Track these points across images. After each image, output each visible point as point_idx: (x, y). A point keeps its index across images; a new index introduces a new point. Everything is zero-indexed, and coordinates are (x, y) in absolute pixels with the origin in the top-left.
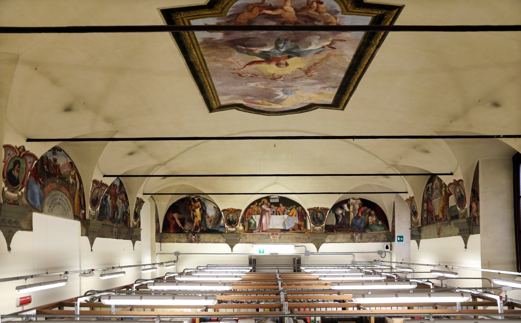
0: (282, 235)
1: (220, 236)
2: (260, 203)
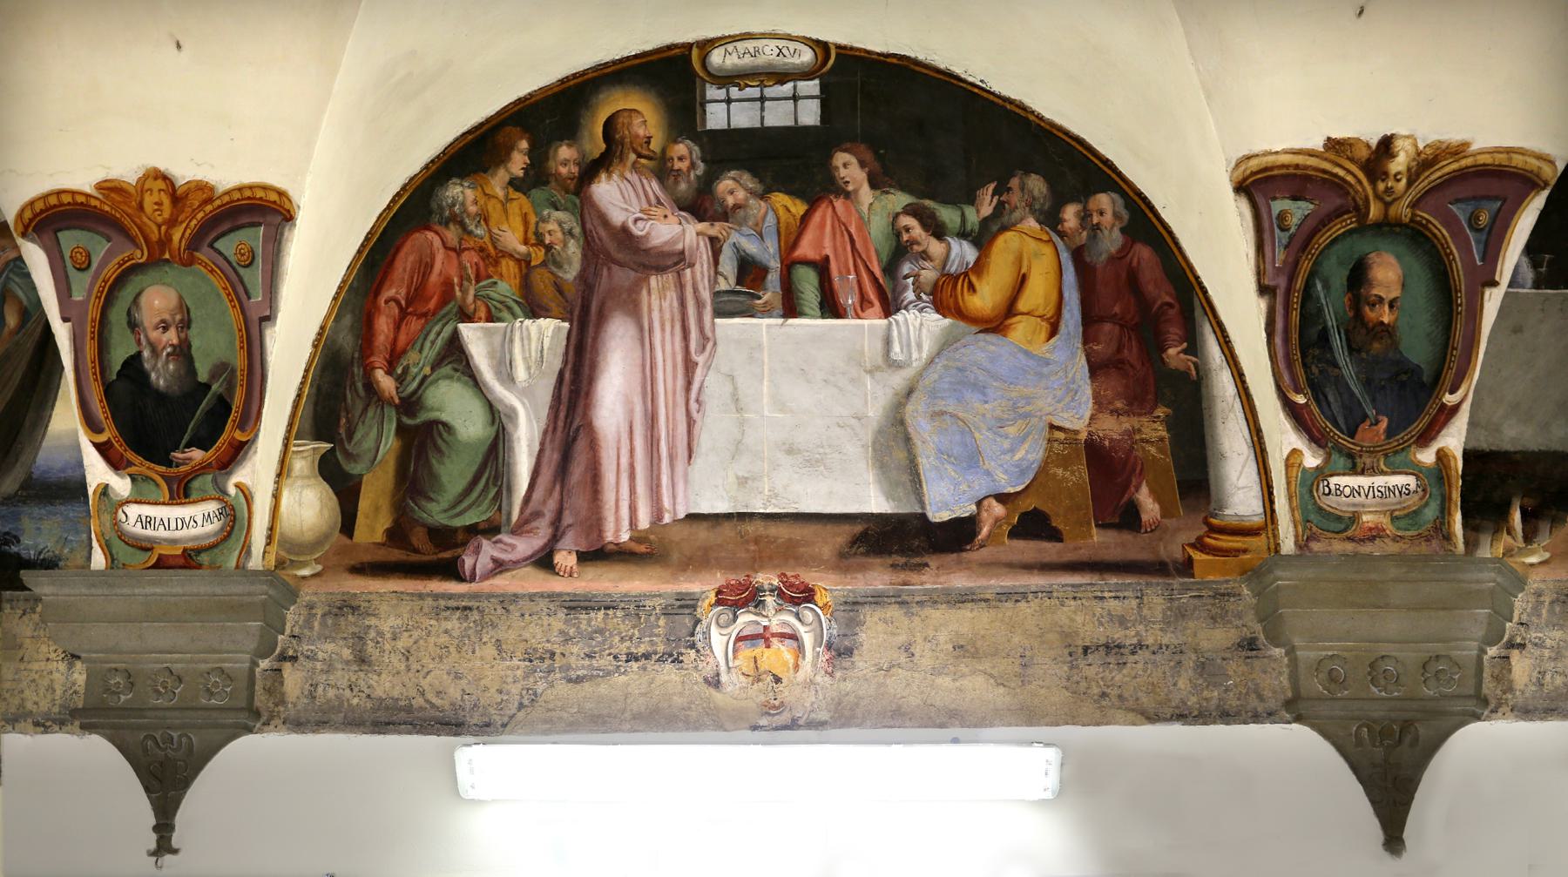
0: (877, 600)
2: (565, 152)
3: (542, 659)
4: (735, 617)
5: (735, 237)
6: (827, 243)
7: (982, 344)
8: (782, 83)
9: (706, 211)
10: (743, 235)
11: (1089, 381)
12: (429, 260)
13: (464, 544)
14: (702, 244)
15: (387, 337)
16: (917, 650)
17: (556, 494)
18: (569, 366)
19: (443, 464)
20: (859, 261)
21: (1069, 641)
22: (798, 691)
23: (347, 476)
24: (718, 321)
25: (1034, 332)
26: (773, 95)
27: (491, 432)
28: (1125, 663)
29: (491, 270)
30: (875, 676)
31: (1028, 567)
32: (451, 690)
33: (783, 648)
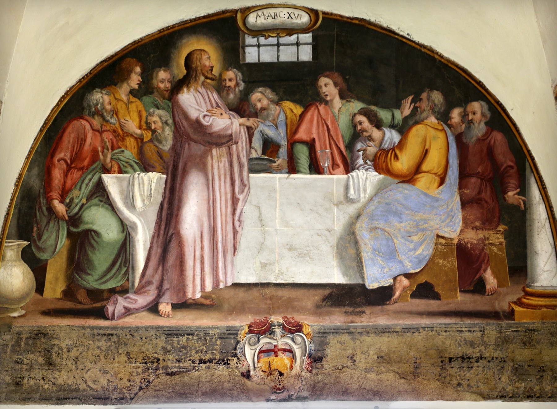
2: (162, 74)
3: (152, 363)
4: (259, 340)
5: (261, 127)
6: (314, 130)
7: (400, 189)
8: (290, 35)
9: (245, 111)
10: (266, 126)
11: (460, 210)
12: (83, 137)
13: (108, 299)
14: (242, 130)
15: (60, 181)
16: (357, 358)
17: (160, 272)
18: (166, 200)
19: (95, 254)
20: (332, 142)
21: (441, 354)
22: (292, 381)
23: (38, 260)
24: (251, 175)
25: (431, 183)
26: (285, 42)
27: (122, 236)
28: (472, 367)
29: (120, 144)
30: (334, 373)
31: (421, 314)
32: (102, 380)
33: (284, 357)
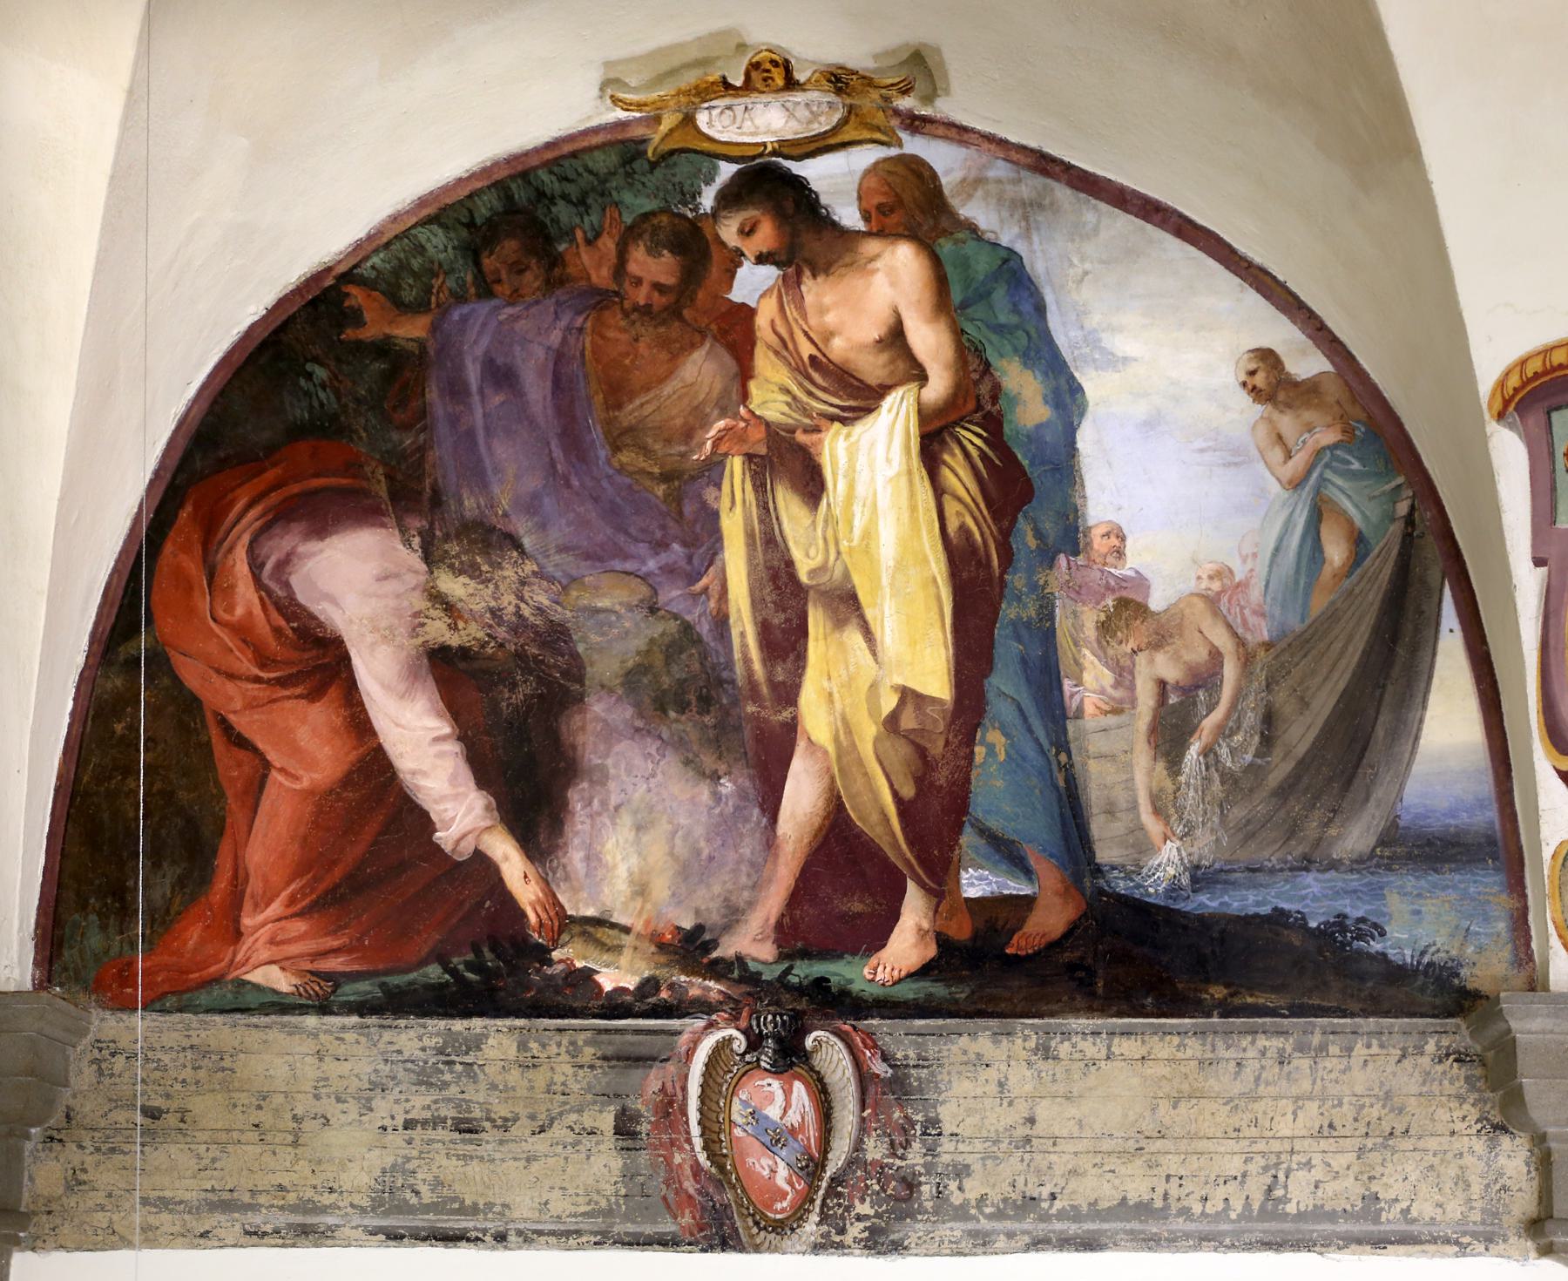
1: (1407, 1079)
